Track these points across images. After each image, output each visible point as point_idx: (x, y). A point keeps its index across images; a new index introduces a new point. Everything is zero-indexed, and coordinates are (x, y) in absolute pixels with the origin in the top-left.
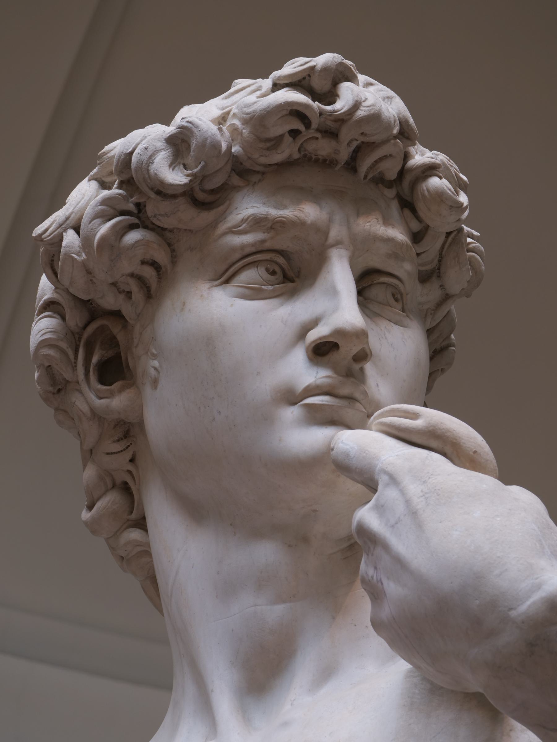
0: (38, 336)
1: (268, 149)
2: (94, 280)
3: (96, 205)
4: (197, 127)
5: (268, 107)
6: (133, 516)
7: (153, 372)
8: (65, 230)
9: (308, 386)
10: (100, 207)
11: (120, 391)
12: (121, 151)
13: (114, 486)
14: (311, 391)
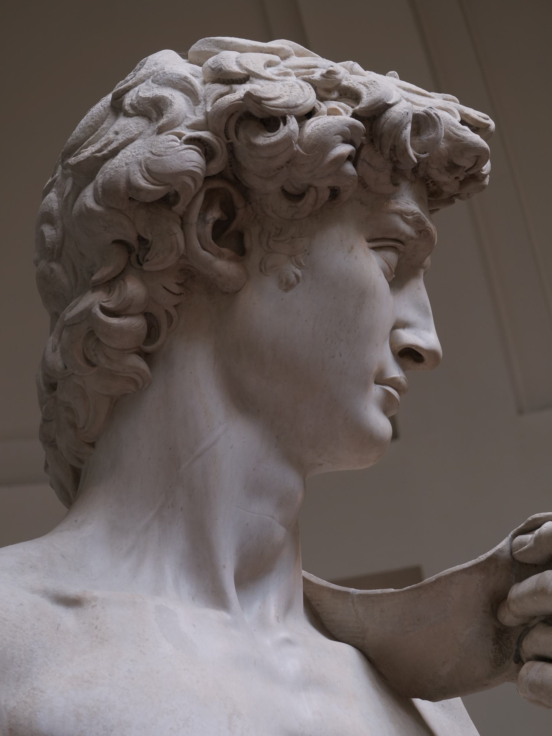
0: (188, 164)
2: (285, 168)
3: (345, 125)
4: (441, 125)
5: (477, 144)
6: (149, 348)
7: (293, 278)
8: (290, 114)
10: (347, 129)
11: (230, 259)
12: (382, 97)
14: (393, 383)
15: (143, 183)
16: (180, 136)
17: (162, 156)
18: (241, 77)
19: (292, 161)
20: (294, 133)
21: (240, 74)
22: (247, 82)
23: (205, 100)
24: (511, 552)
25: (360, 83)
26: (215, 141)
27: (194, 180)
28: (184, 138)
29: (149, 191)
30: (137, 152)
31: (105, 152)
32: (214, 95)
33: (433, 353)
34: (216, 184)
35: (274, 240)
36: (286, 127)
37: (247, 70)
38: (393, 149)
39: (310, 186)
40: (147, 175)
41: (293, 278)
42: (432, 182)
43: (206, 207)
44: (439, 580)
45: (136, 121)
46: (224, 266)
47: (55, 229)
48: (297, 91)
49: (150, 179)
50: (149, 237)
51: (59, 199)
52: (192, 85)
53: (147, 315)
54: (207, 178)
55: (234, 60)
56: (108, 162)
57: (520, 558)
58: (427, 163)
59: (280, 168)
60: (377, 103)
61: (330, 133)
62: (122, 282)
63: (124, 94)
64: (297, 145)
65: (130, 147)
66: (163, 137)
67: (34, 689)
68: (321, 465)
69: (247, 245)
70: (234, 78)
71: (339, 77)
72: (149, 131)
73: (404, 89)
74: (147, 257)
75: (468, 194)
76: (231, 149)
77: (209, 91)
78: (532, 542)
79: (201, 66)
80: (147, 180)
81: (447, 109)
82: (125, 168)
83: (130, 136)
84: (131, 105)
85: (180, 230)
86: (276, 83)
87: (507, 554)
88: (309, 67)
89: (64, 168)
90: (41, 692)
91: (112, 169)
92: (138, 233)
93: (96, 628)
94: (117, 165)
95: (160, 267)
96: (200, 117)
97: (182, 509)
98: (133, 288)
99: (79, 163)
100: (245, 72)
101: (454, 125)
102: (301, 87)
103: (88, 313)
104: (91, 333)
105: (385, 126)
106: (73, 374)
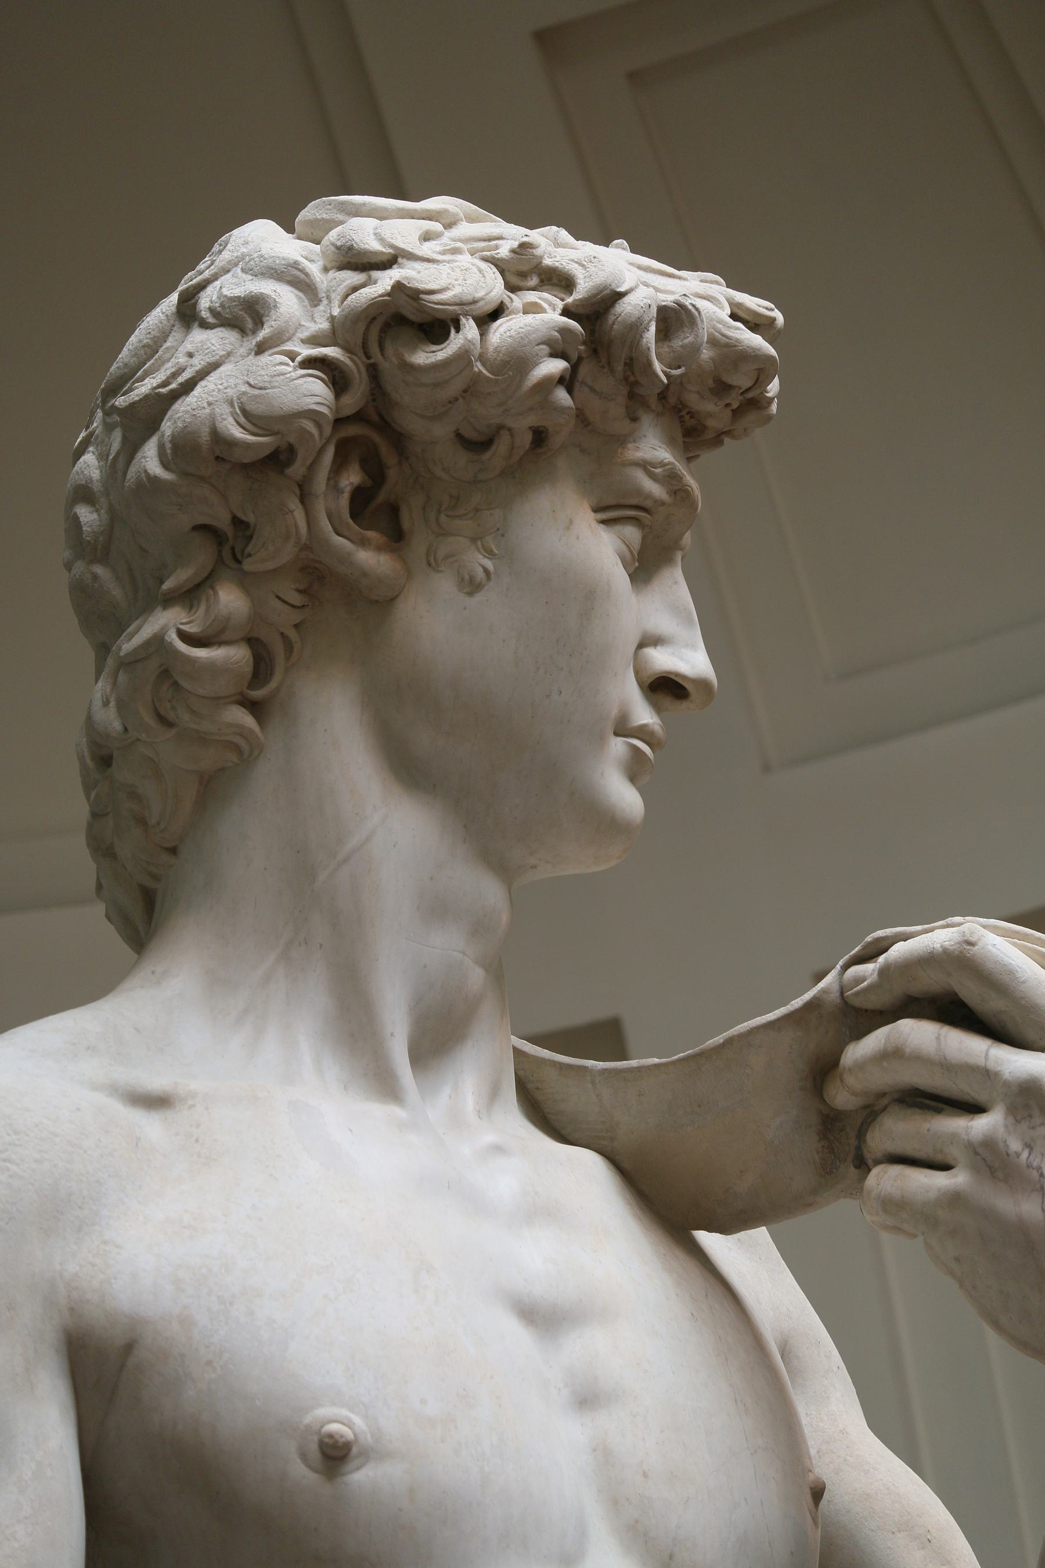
0: (308, 400)
1: (710, 389)
2: (461, 400)
3: (553, 328)
4: (702, 321)
5: (759, 350)
6: (257, 694)
7: (480, 574)
8: (465, 315)
9: (645, 726)
10: (556, 334)
11: (379, 549)
12: (609, 282)
13: (243, 639)
14: (643, 733)
15: (238, 433)
16: (292, 356)
17: (265, 388)
18: (384, 258)
19: (472, 388)
20: (474, 344)
21: (382, 253)
22: (395, 266)
23: (328, 297)
24: (842, 993)
25: (573, 260)
26: (348, 362)
27: (319, 426)
28: (299, 359)
29: (247, 446)
30: (225, 385)
31: (173, 386)
32: (342, 289)
33: (703, 684)
34: (352, 430)
35: (447, 516)
36: (460, 336)
37: (392, 246)
38: (630, 363)
39: (501, 427)
40: (242, 420)
41: (480, 574)
42: (688, 413)
43: (339, 466)
44: (729, 1042)
45: (221, 334)
46: (371, 559)
47: (97, 511)
48: (474, 278)
49: (249, 426)
50: (250, 518)
51: (102, 463)
52: (307, 275)
53: (252, 642)
54: (339, 422)
55: (372, 232)
56: (179, 402)
57: (857, 1002)
58: (681, 383)
59: (454, 401)
60: (601, 291)
61: (530, 342)
62: (211, 592)
63: (198, 292)
64: (479, 364)
65: (213, 377)
66: (265, 358)
67: (105, 1243)
68: (534, 867)
69: (406, 524)
70: (373, 260)
71: (538, 252)
72: (243, 350)
73: (640, 267)
74: (249, 549)
75: (745, 430)
76: (374, 372)
77: (334, 283)
78: (875, 975)
79: (318, 243)
80: (244, 428)
81: (710, 297)
82: (207, 411)
83: (212, 360)
84: (211, 310)
85: (300, 506)
86: (440, 267)
87: (835, 995)
88: (490, 239)
89: (107, 414)
90: (117, 1247)
91: (187, 412)
92: (232, 513)
93: (197, 1141)
94: (195, 406)
95: (270, 566)
96: (324, 325)
97: (321, 946)
98: (230, 600)
99: (133, 405)
100: (391, 251)
101: (721, 322)
102: (480, 271)
103: (158, 642)
104: (165, 674)
105: (615, 327)
106: (138, 740)
